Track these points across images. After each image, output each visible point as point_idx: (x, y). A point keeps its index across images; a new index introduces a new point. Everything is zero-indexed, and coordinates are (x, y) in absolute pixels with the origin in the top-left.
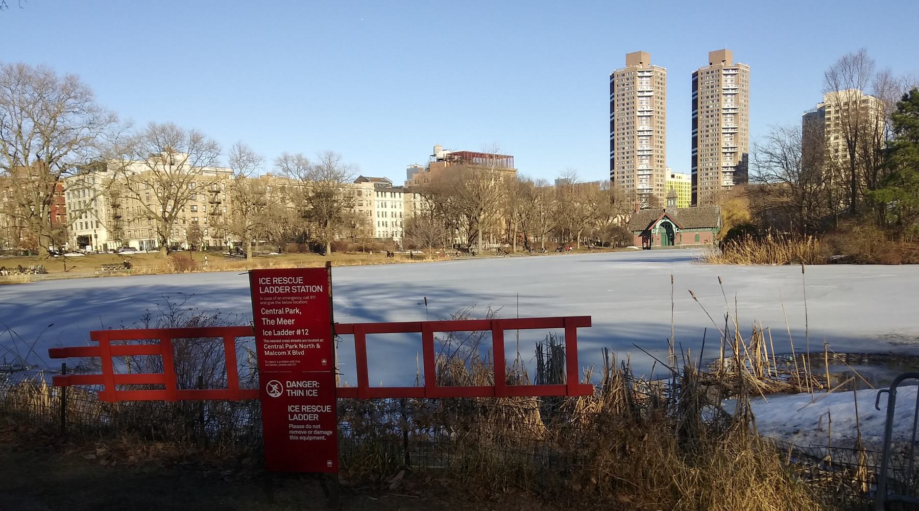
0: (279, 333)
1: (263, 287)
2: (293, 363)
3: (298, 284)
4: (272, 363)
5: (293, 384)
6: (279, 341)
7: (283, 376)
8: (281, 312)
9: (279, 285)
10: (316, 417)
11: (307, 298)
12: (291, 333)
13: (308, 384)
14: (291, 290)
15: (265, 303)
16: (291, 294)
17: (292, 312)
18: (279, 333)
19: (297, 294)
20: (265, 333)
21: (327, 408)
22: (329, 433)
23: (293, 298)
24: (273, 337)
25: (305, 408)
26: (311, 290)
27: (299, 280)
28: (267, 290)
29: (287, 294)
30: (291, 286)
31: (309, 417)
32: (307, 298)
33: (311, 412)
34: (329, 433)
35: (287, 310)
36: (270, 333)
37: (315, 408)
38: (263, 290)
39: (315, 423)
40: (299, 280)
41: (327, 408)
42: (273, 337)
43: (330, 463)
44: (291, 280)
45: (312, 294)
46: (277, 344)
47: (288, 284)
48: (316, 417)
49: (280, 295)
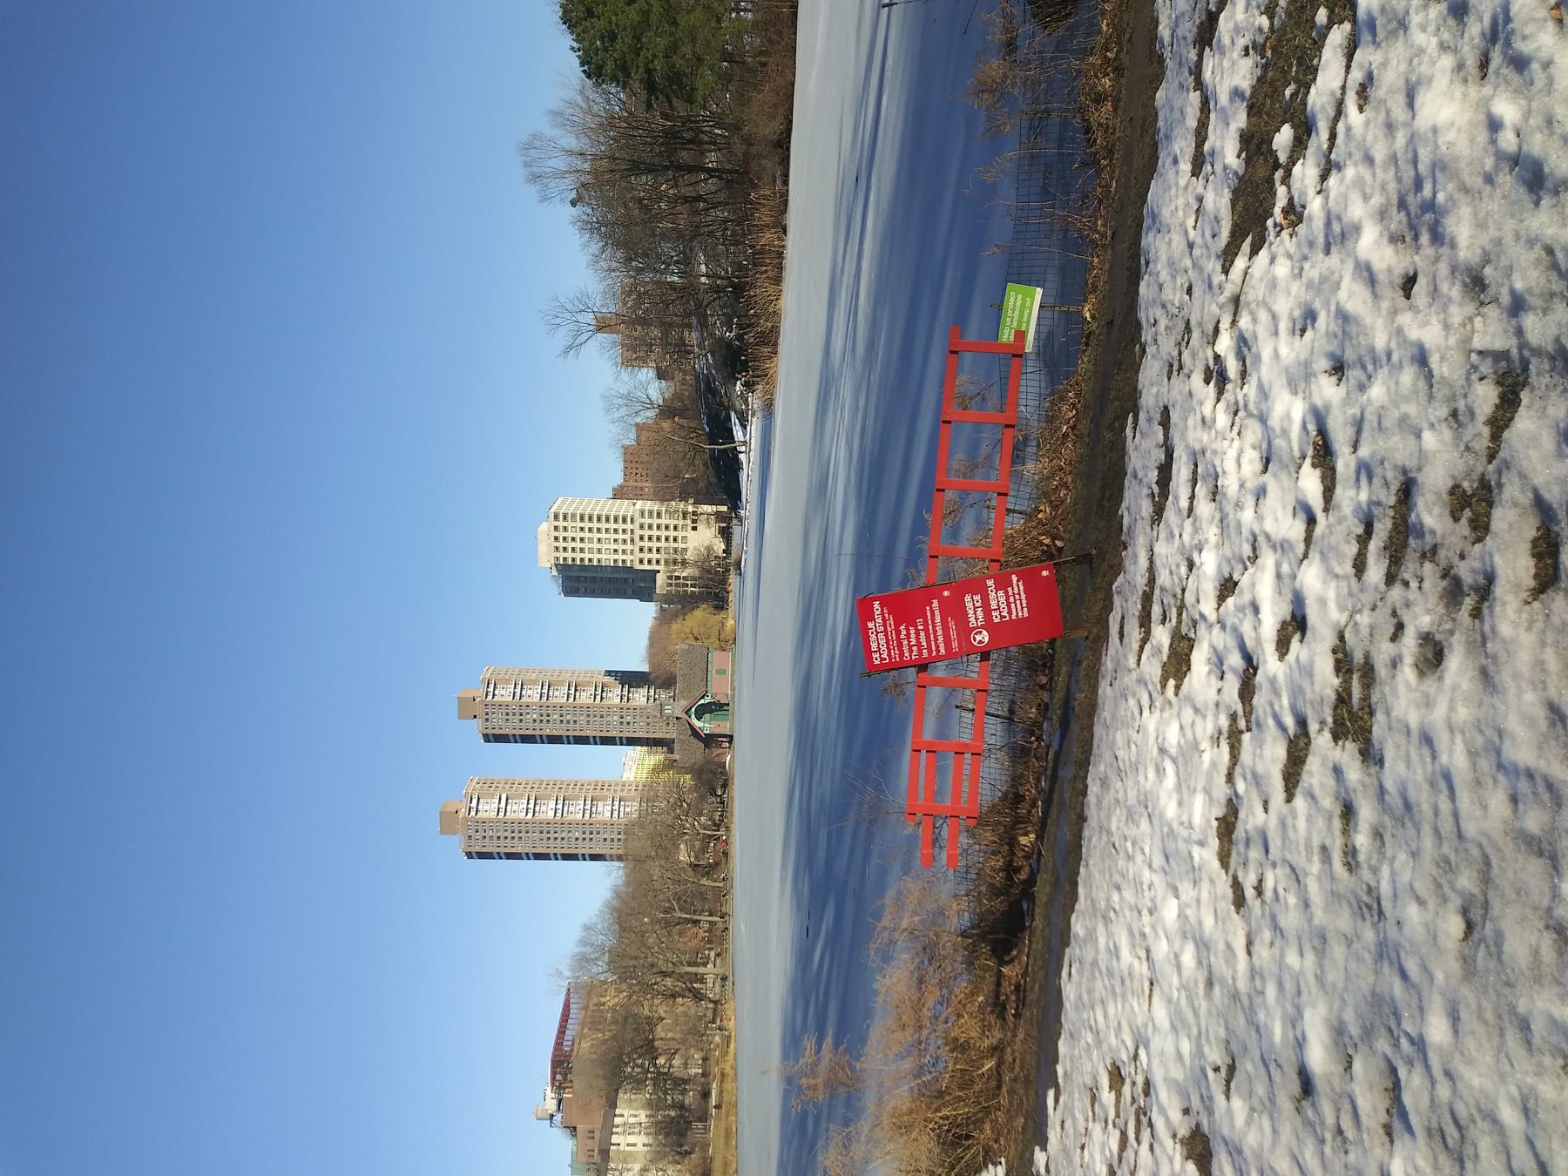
2: (952, 624)
4: (955, 644)
5: (972, 620)
7: (965, 631)
10: (1001, 593)
13: (969, 605)
21: (990, 583)
22: (1014, 578)
25: (994, 605)
31: (1002, 600)
33: (996, 598)
34: (1014, 578)
37: (992, 595)
39: (1006, 593)
41: (990, 583)
43: (1045, 573)
48: (1001, 593)
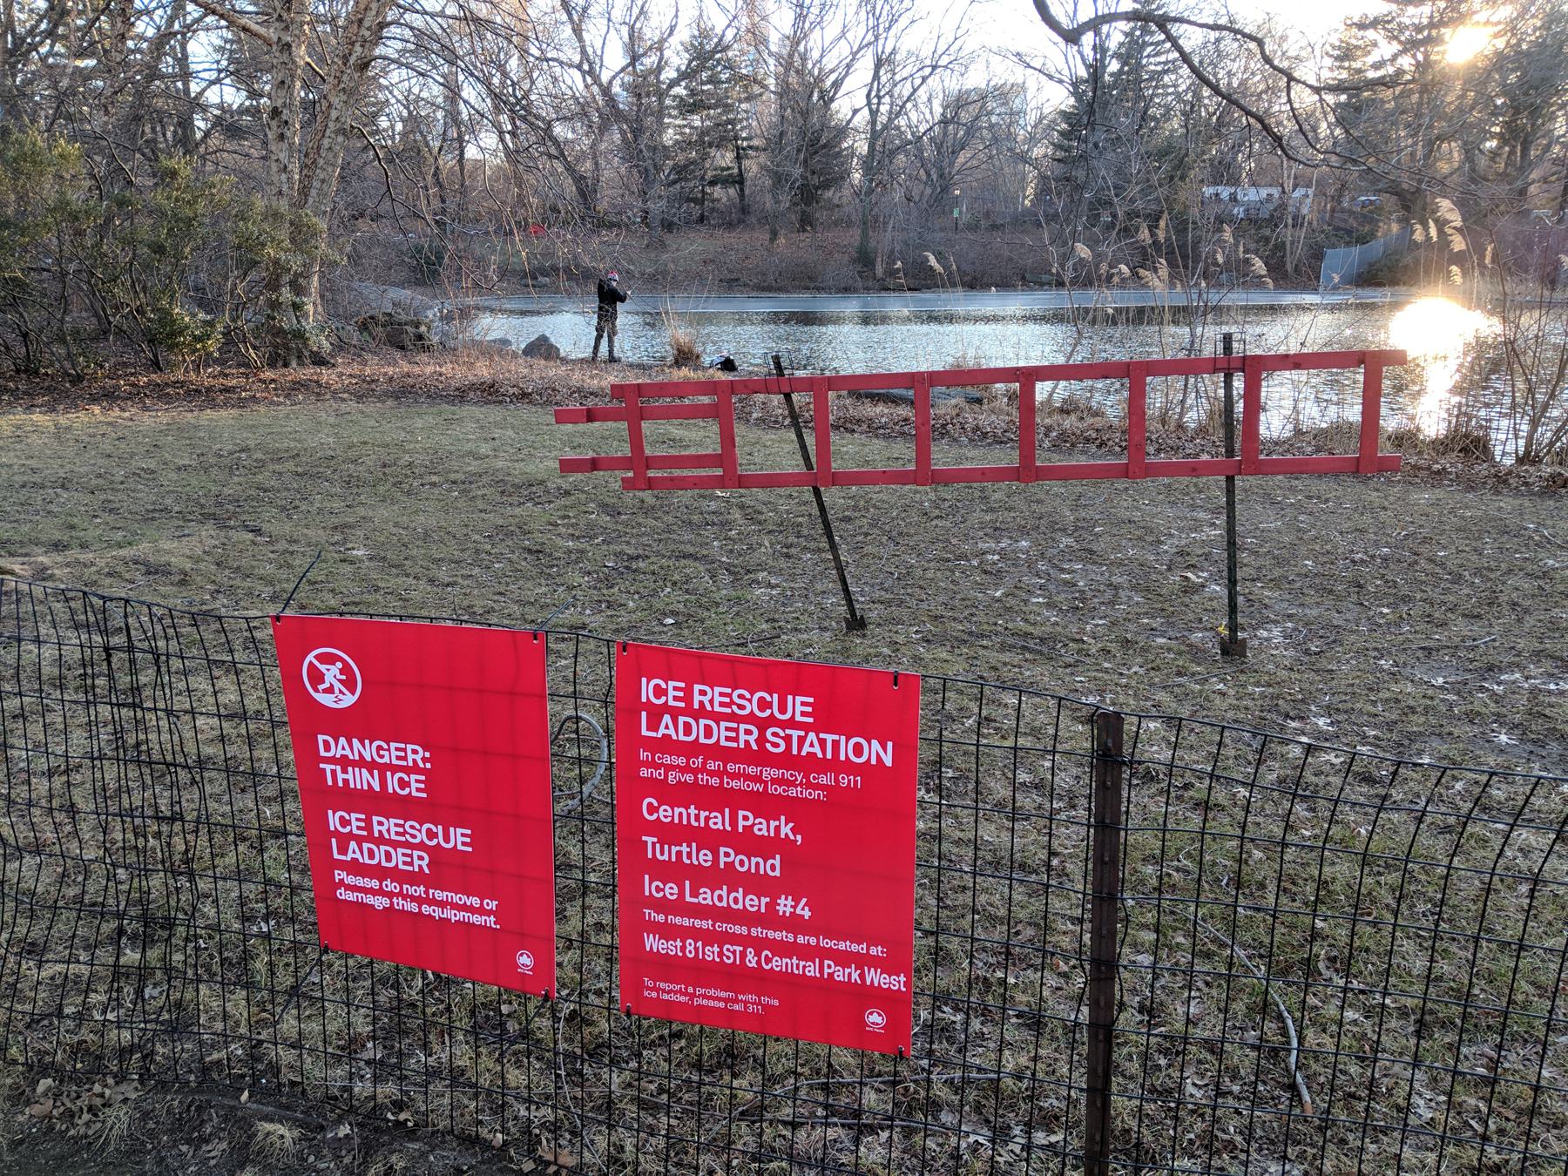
0: (706, 897)
1: (656, 715)
3: (792, 723)
6: (706, 924)
8: (718, 822)
9: (718, 717)
11: (824, 780)
12: (753, 903)
14: (762, 740)
15: (658, 774)
16: (761, 756)
17: (762, 828)
18: (706, 897)
19: (786, 760)
20: (650, 887)
23: (769, 773)
24: (679, 907)
26: (846, 750)
27: (799, 706)
28: (666, 727)
29: (745, 755)
30: (763, 725)
32: (824, 780)
35: (745, 819)
36: (671, 891)
38: (653, 726)
40: (799, 706)
42: (679, 907)
44: (763, 705)
45: (849, 767)
46: (695, 934)
47: (751, 719)
49: (716, 752)
